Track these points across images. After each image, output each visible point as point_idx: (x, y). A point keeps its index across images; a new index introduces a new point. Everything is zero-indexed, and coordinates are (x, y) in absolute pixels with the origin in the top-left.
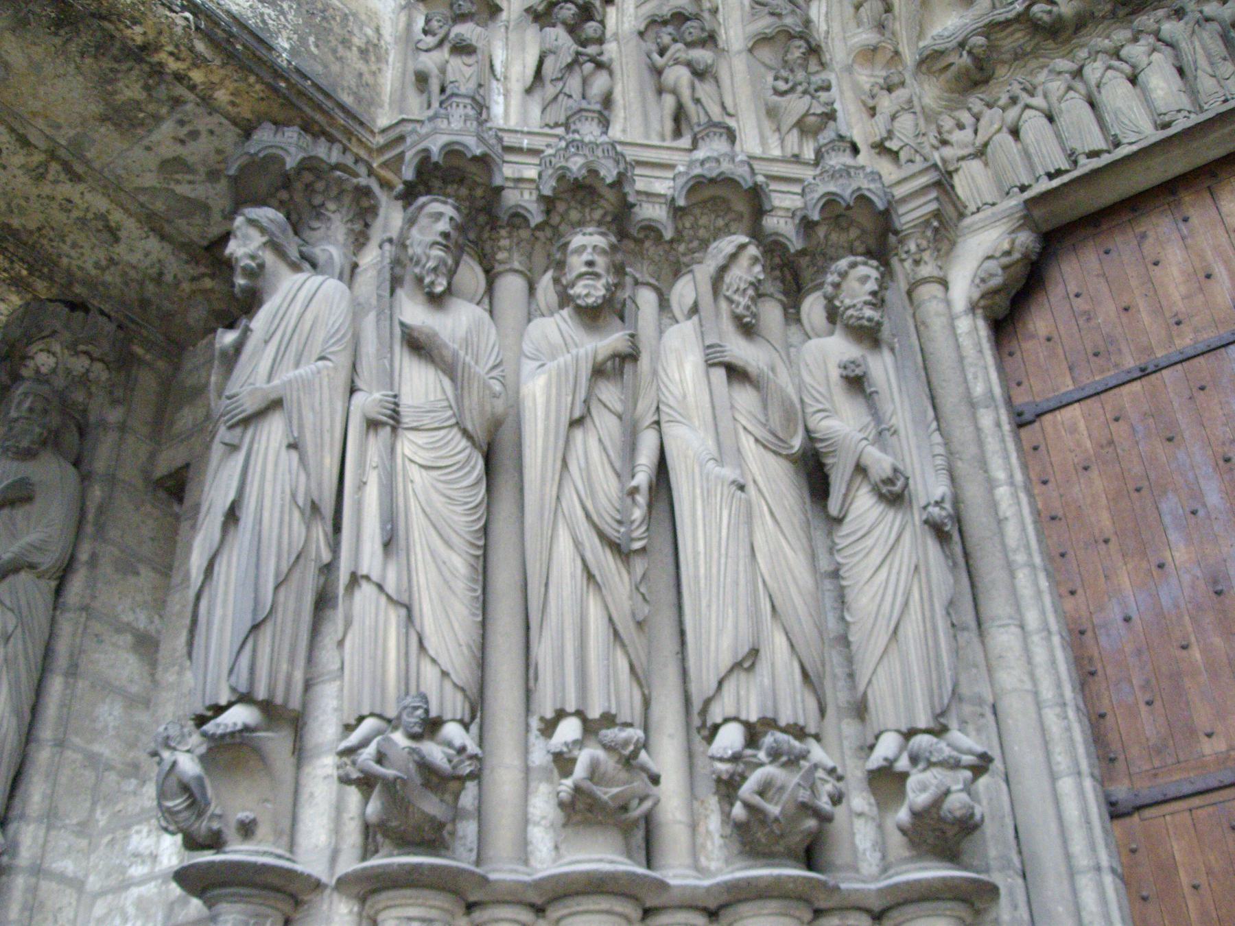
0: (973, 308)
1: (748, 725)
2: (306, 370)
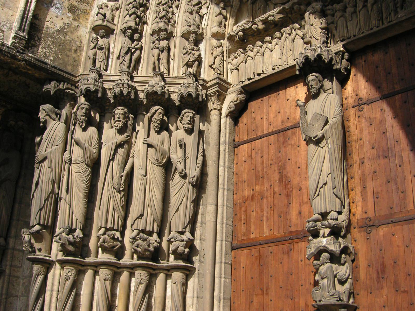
1: (139, 230)
2: (54, 148)
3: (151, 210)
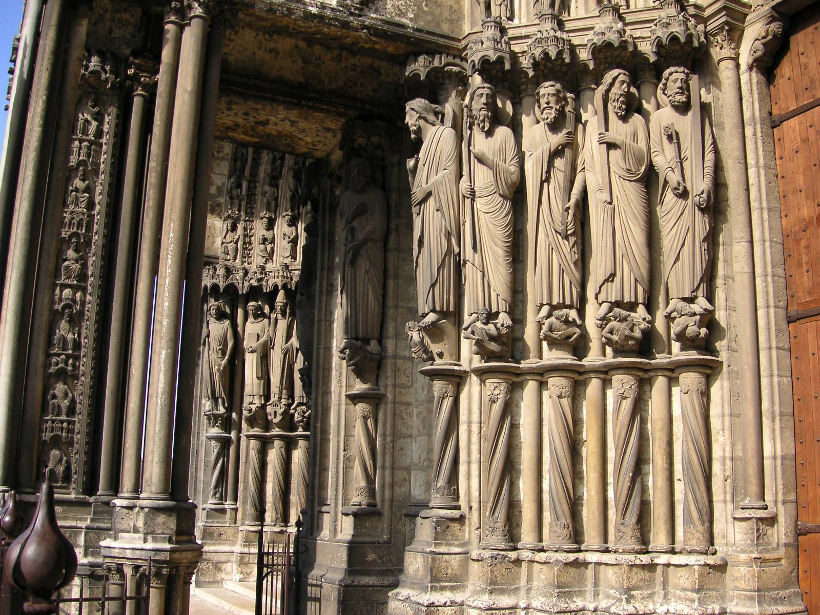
1: (610, 302)
2: (440, 174)
3: (629, 263)
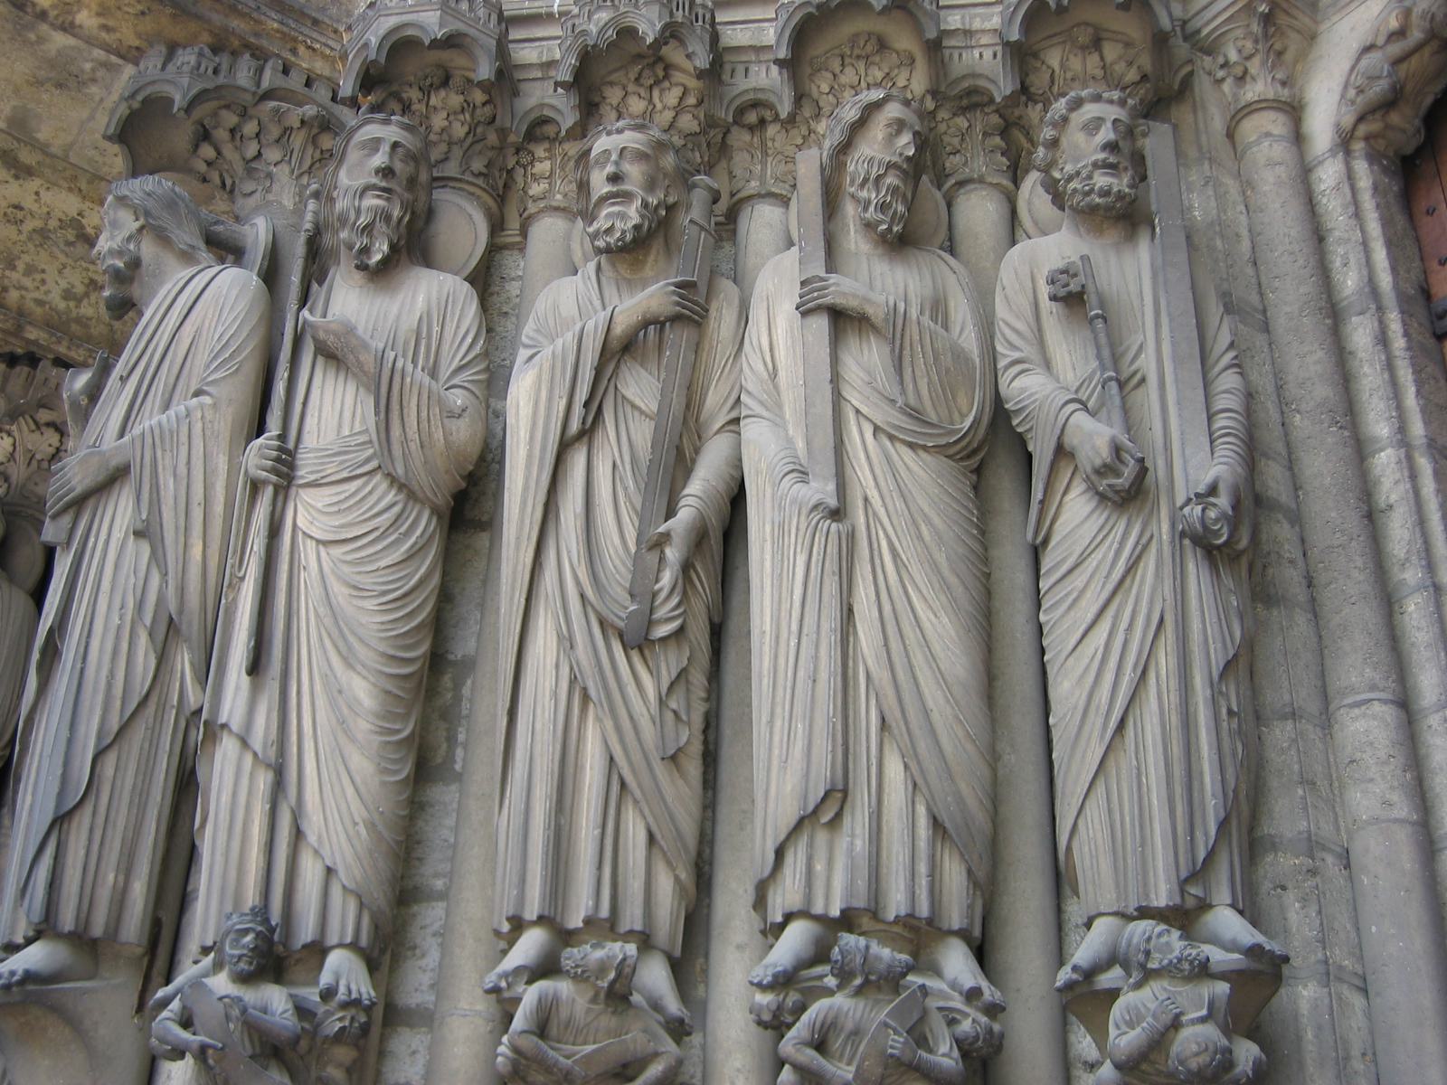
0: (1344, 142)
1: (822, 919)
